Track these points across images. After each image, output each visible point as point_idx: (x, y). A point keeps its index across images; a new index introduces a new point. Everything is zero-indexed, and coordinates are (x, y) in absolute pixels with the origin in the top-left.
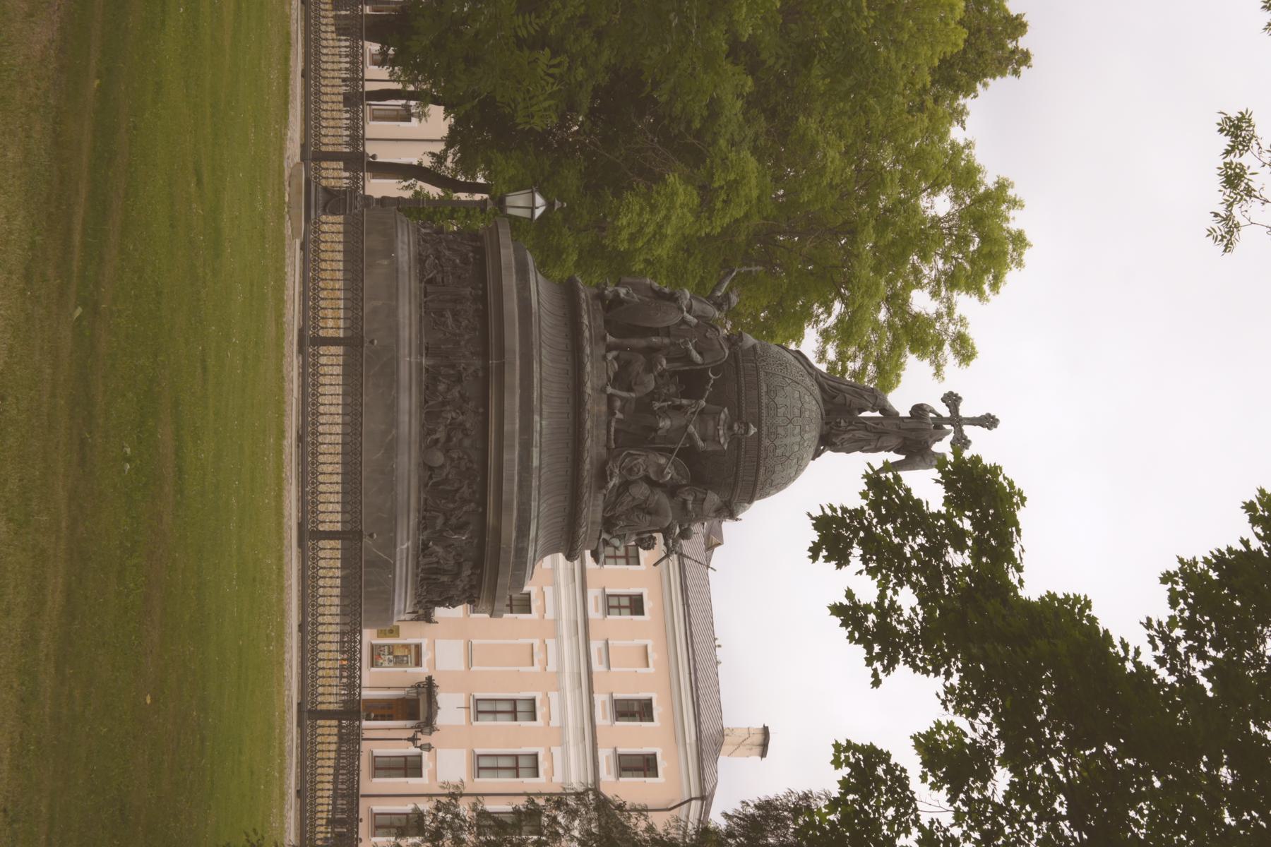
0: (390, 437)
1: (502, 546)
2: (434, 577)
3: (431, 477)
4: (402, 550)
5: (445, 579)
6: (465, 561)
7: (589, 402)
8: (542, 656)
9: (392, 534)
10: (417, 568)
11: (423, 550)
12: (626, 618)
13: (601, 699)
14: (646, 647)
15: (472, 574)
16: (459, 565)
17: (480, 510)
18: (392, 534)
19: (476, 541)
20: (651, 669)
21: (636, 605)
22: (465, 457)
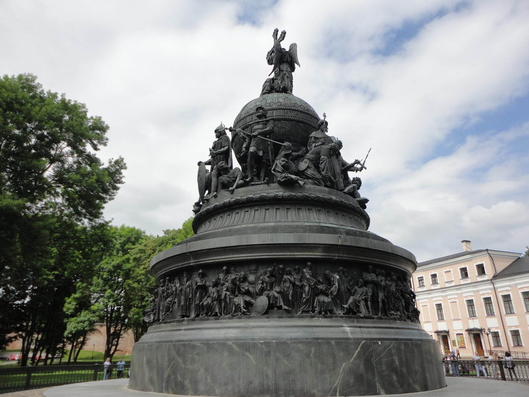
0: (235, 347)
1: (340, 243)
2: (380, 304)
3: (280, 308)
4: (352, 333)
5: (381, 295)
6: (362, 278)
7: (236, 198)
8: (453, 299)
9: (333, 342)
10: (373, 318)
11: (354, 313)
12: (438, 278)
13: (463, 282)
14: (445, 272)
15: (375, 273)
16: (366, 283)
17: (309, 263)
18: (333, 342)
19: (341, 268)
20: (451, 270)
21: (434, 276)
22: (261, 278)
